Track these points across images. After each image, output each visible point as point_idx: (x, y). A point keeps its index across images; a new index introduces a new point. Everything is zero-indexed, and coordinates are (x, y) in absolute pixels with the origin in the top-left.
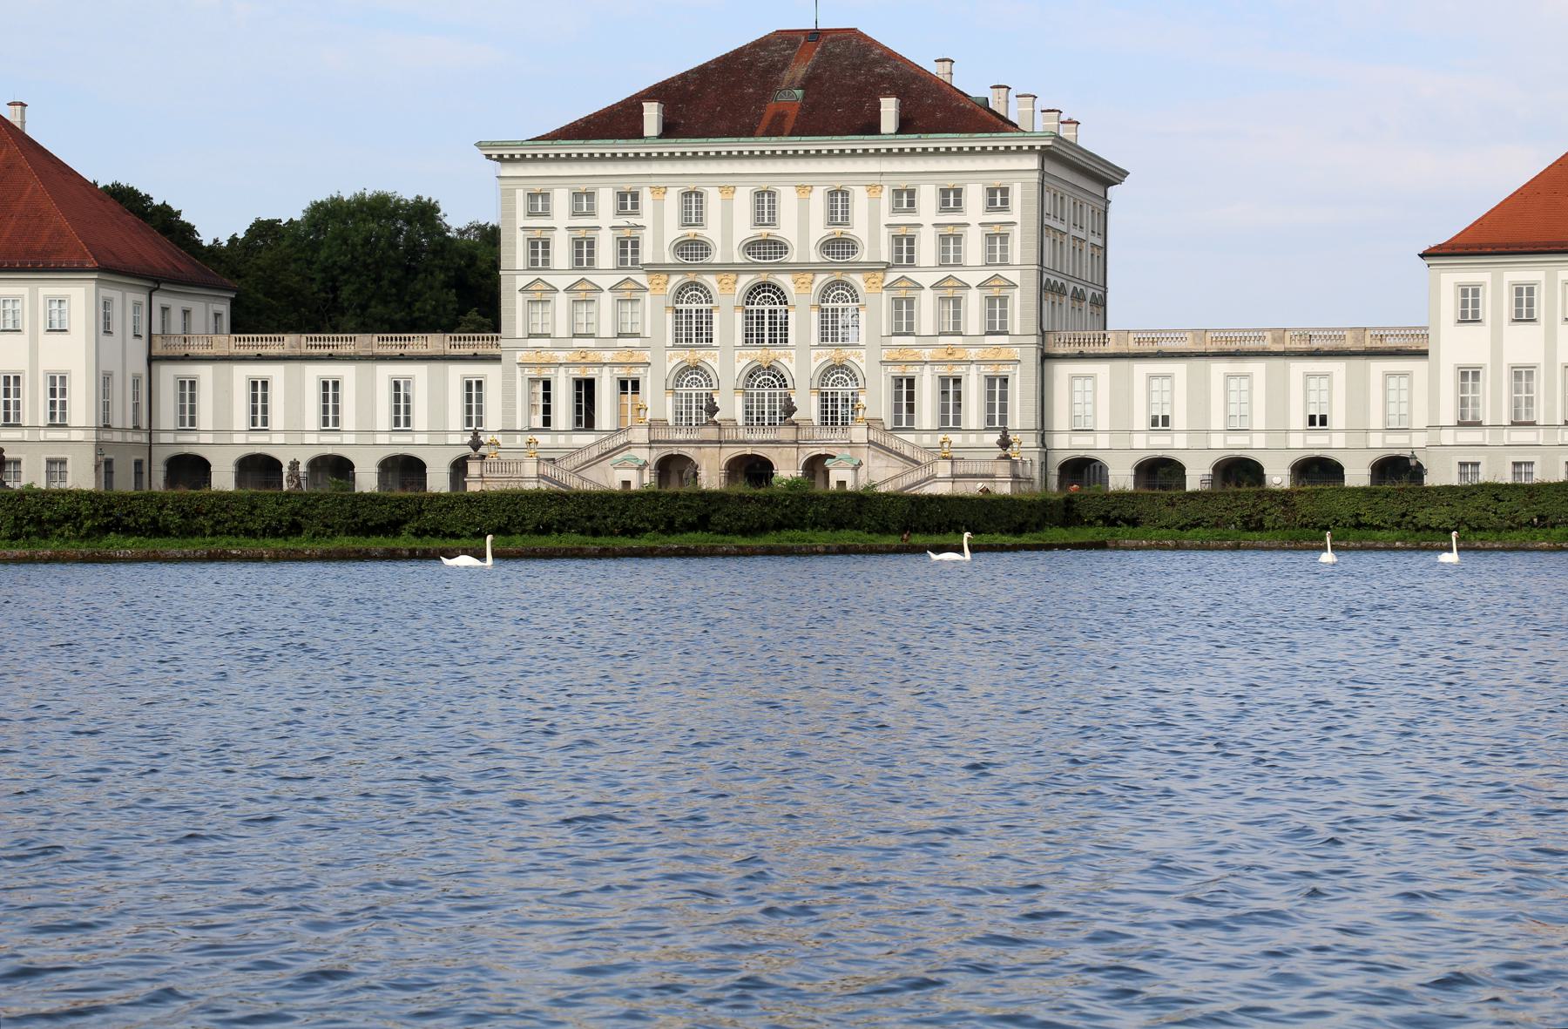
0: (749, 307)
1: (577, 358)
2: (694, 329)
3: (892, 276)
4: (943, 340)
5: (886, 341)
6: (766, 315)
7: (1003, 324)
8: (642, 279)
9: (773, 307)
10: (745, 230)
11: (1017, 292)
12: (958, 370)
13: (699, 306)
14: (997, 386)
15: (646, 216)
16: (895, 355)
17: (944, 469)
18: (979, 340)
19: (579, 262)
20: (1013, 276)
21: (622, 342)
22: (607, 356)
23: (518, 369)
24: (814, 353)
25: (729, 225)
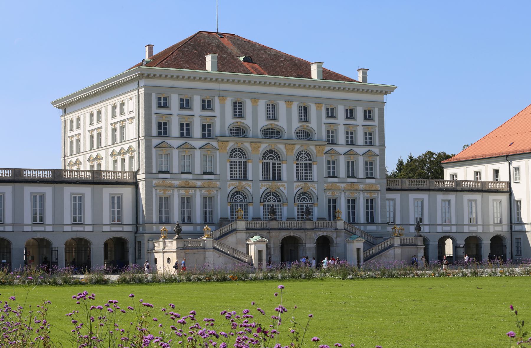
0: (264, 161)
1: (183, 184)
2: (239, 173)
3: (328, 148)
4: (350, 180)
5: (326, 180)
6: (271, 165)
7: (371, 174)
8: (214, 143)
9: (274, 162)
10: (263, 122)
11: (378, 158)
12: (356, 195)
13: (240, 160)
14: (370, 204)
15: (217, 112)
16: (330, 187)
17: (397, 241)
18: (363, 181)
19: (182, 134)
20: (376, 150)
21: (206, 177)
22: (199, 183)
23: (154, 190)
24: (295, 184)
25: (256, 119)
